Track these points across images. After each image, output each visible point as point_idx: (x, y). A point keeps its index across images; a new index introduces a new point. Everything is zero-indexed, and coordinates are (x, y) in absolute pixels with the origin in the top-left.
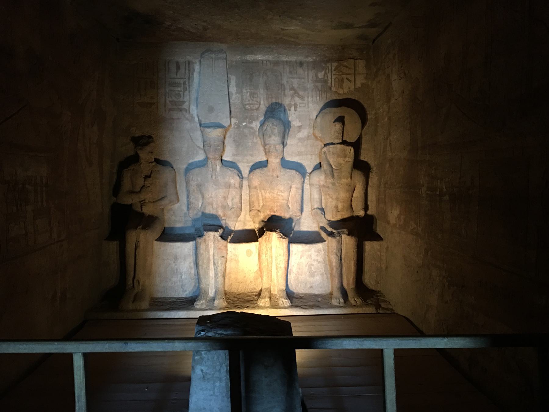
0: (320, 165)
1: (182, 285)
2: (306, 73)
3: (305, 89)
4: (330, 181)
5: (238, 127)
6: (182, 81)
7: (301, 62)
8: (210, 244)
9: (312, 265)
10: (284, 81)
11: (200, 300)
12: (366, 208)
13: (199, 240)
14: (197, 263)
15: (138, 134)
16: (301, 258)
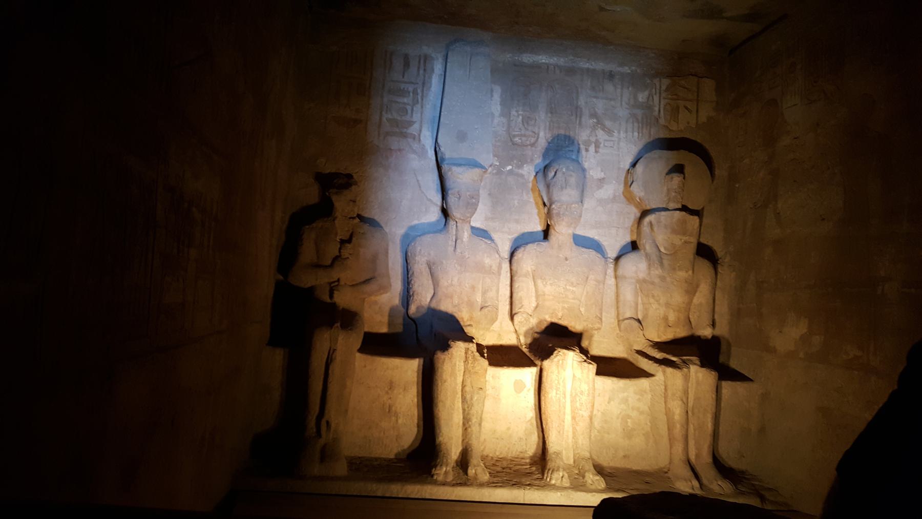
0: (634, 246)
2: (619, 90)
4: (657, 272)
6: (411, 89)
10: (582, 102)
12: (713, 325)
15: (329, 169)
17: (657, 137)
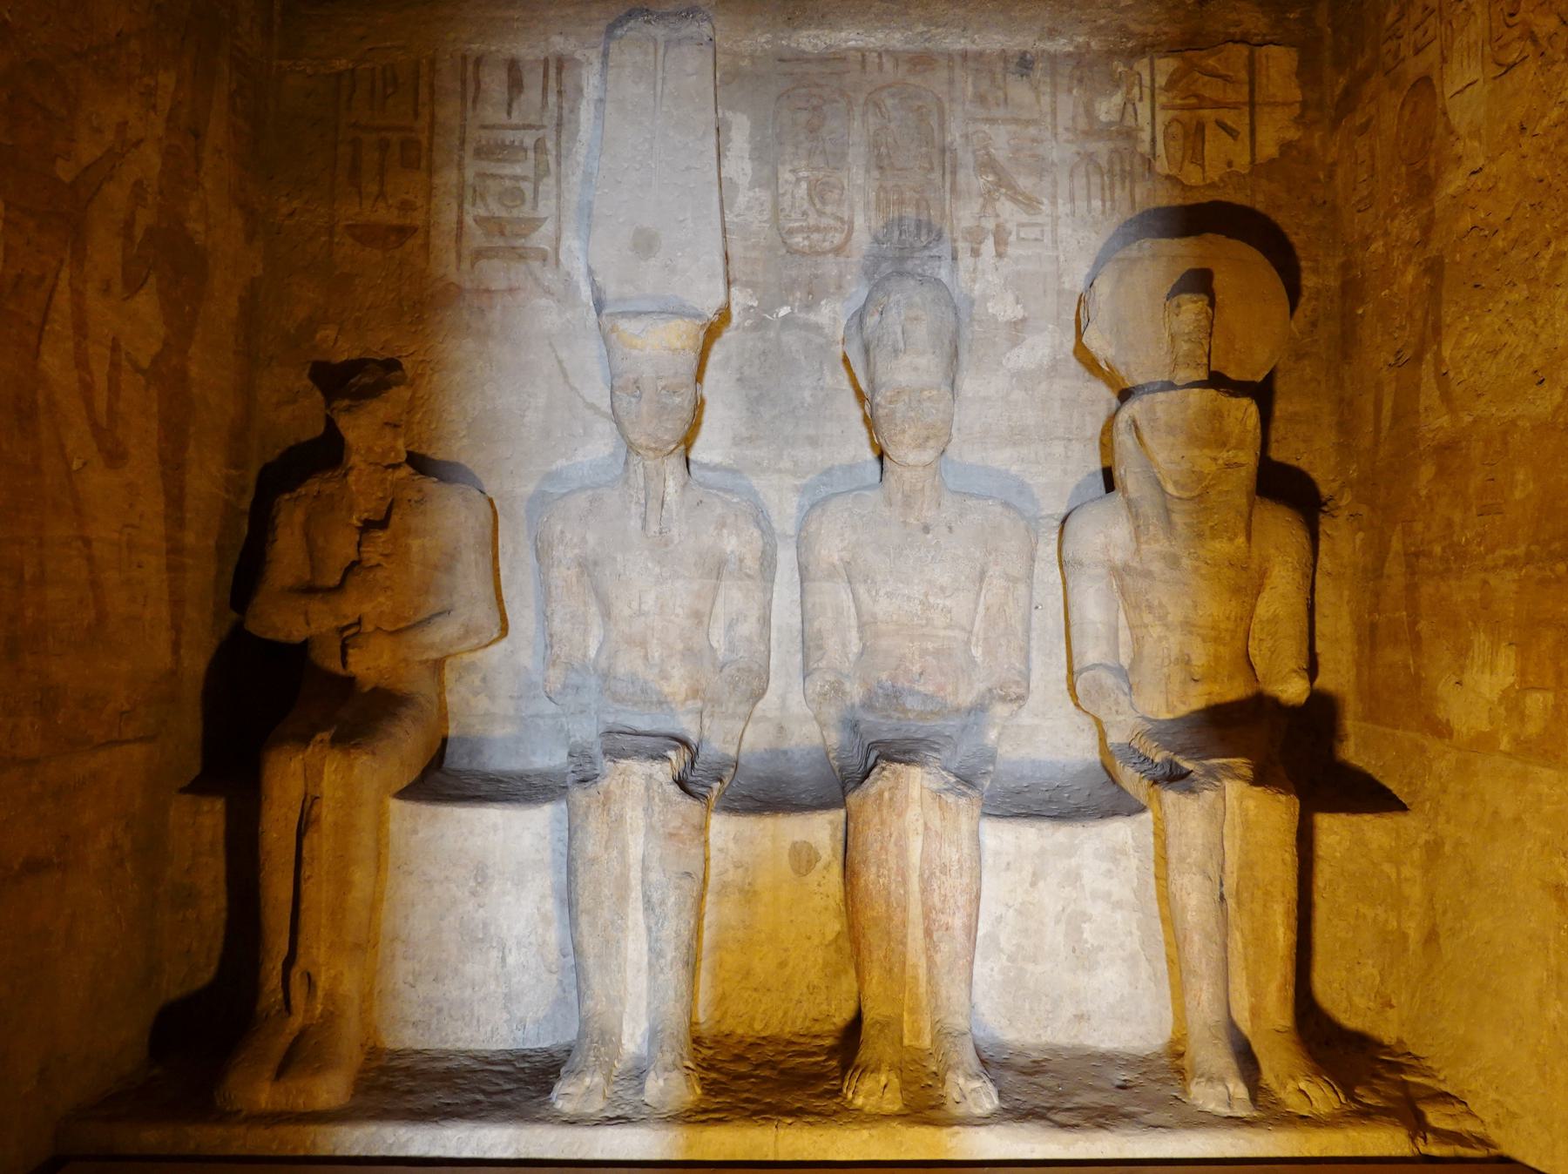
1: (508, 997)
2: (1046, 100)
3: (1040, 167)
4: (1157, 547)
5: (760, 325)
7: (1025, 53)
8: (629, 813)
9: (1085, 917)
10: (954, 135)
11: (579, 1073)
12: (1312, 669)
13: (578, 795)
14: (570, 901)
15: (345, 352)
16: (1033, 884)
17: (1153, 205)
